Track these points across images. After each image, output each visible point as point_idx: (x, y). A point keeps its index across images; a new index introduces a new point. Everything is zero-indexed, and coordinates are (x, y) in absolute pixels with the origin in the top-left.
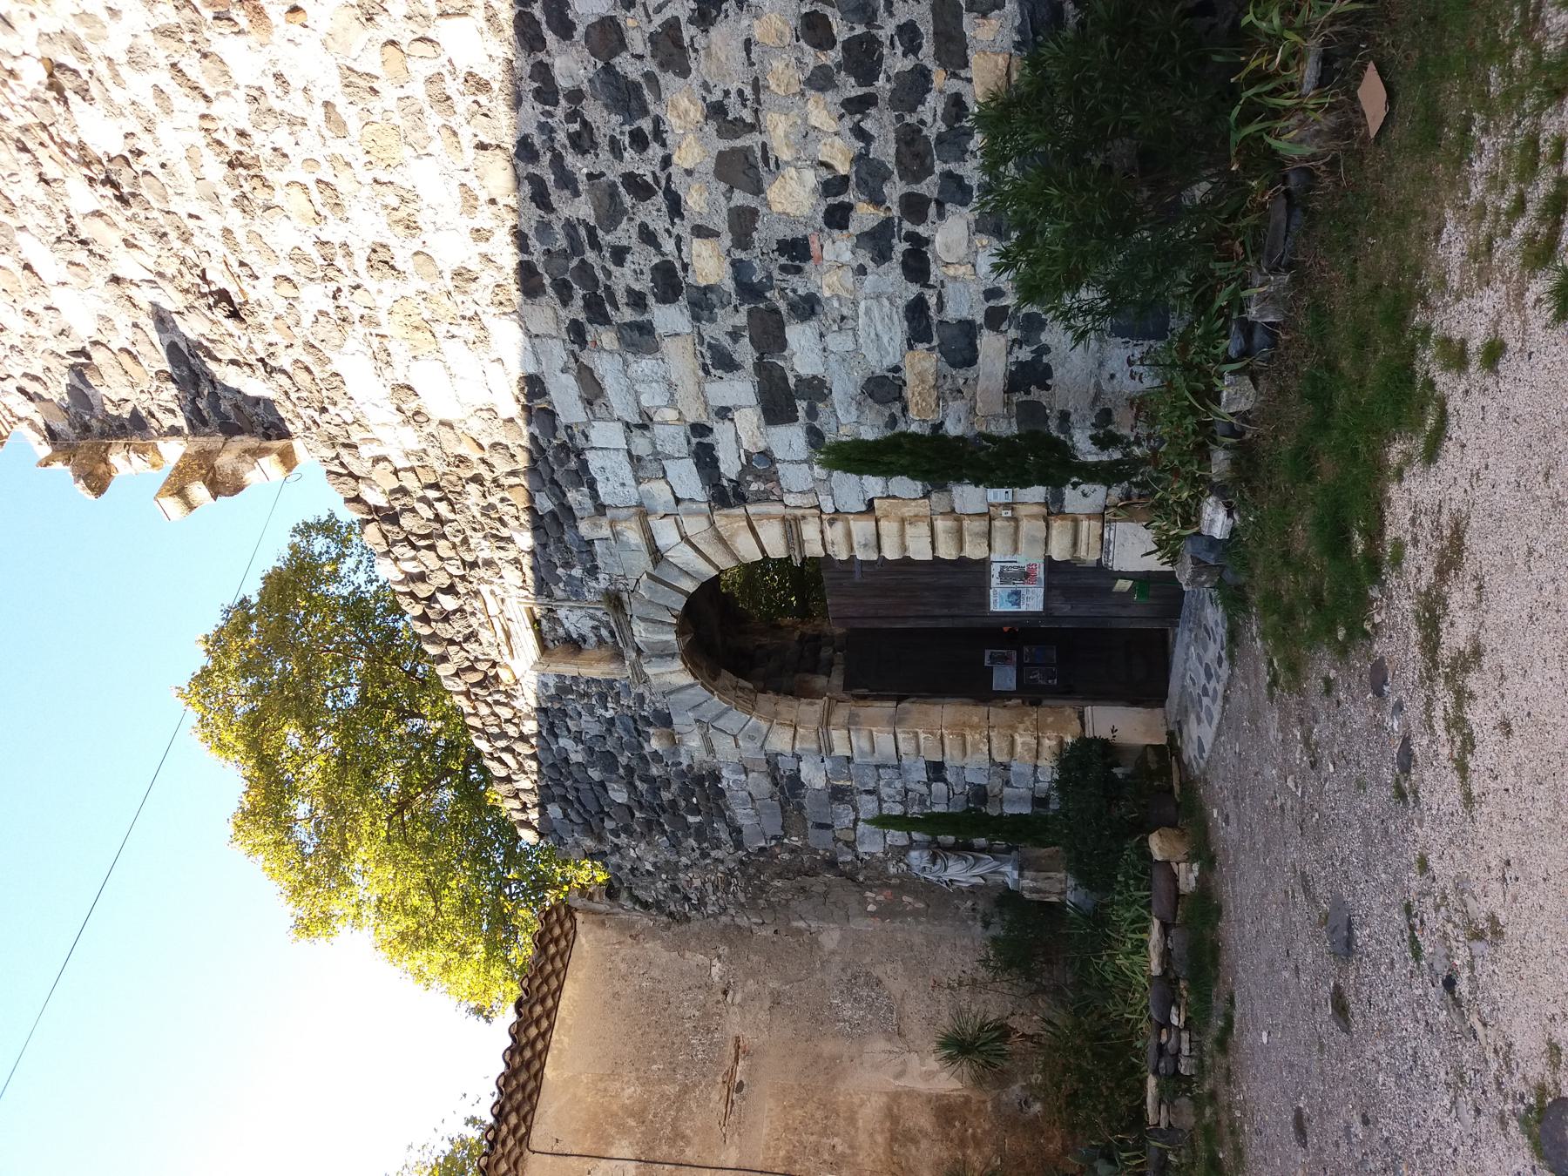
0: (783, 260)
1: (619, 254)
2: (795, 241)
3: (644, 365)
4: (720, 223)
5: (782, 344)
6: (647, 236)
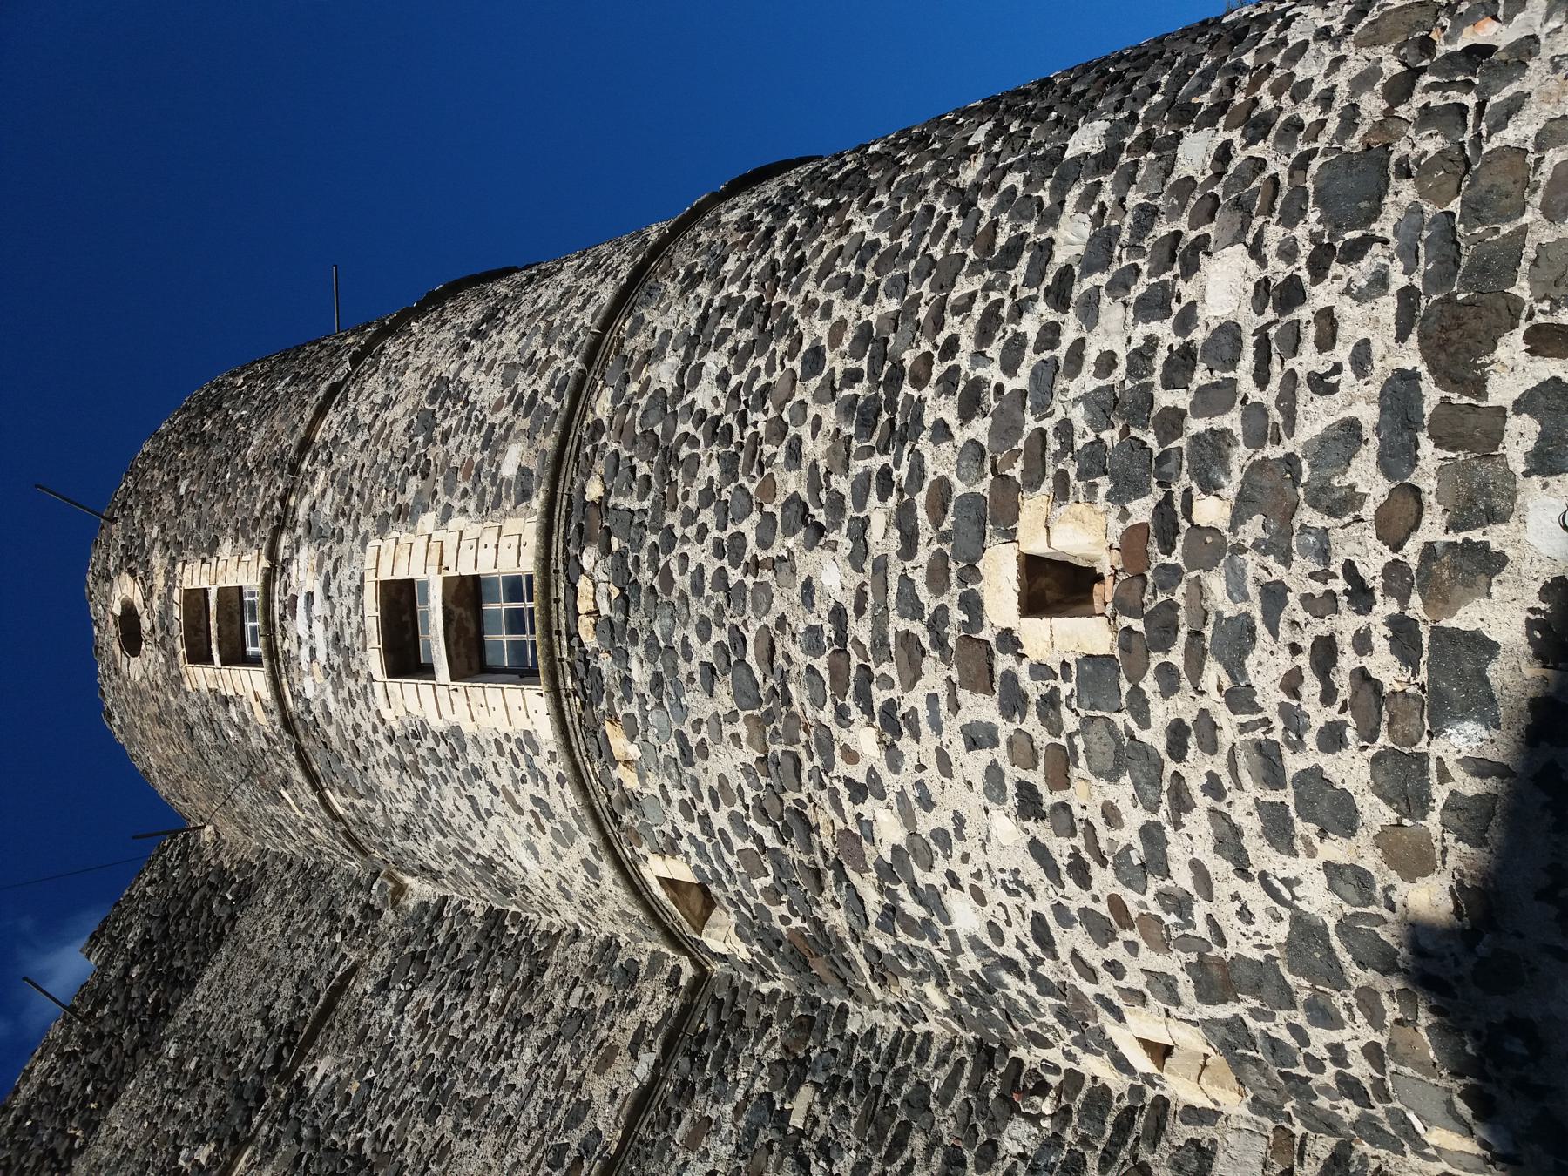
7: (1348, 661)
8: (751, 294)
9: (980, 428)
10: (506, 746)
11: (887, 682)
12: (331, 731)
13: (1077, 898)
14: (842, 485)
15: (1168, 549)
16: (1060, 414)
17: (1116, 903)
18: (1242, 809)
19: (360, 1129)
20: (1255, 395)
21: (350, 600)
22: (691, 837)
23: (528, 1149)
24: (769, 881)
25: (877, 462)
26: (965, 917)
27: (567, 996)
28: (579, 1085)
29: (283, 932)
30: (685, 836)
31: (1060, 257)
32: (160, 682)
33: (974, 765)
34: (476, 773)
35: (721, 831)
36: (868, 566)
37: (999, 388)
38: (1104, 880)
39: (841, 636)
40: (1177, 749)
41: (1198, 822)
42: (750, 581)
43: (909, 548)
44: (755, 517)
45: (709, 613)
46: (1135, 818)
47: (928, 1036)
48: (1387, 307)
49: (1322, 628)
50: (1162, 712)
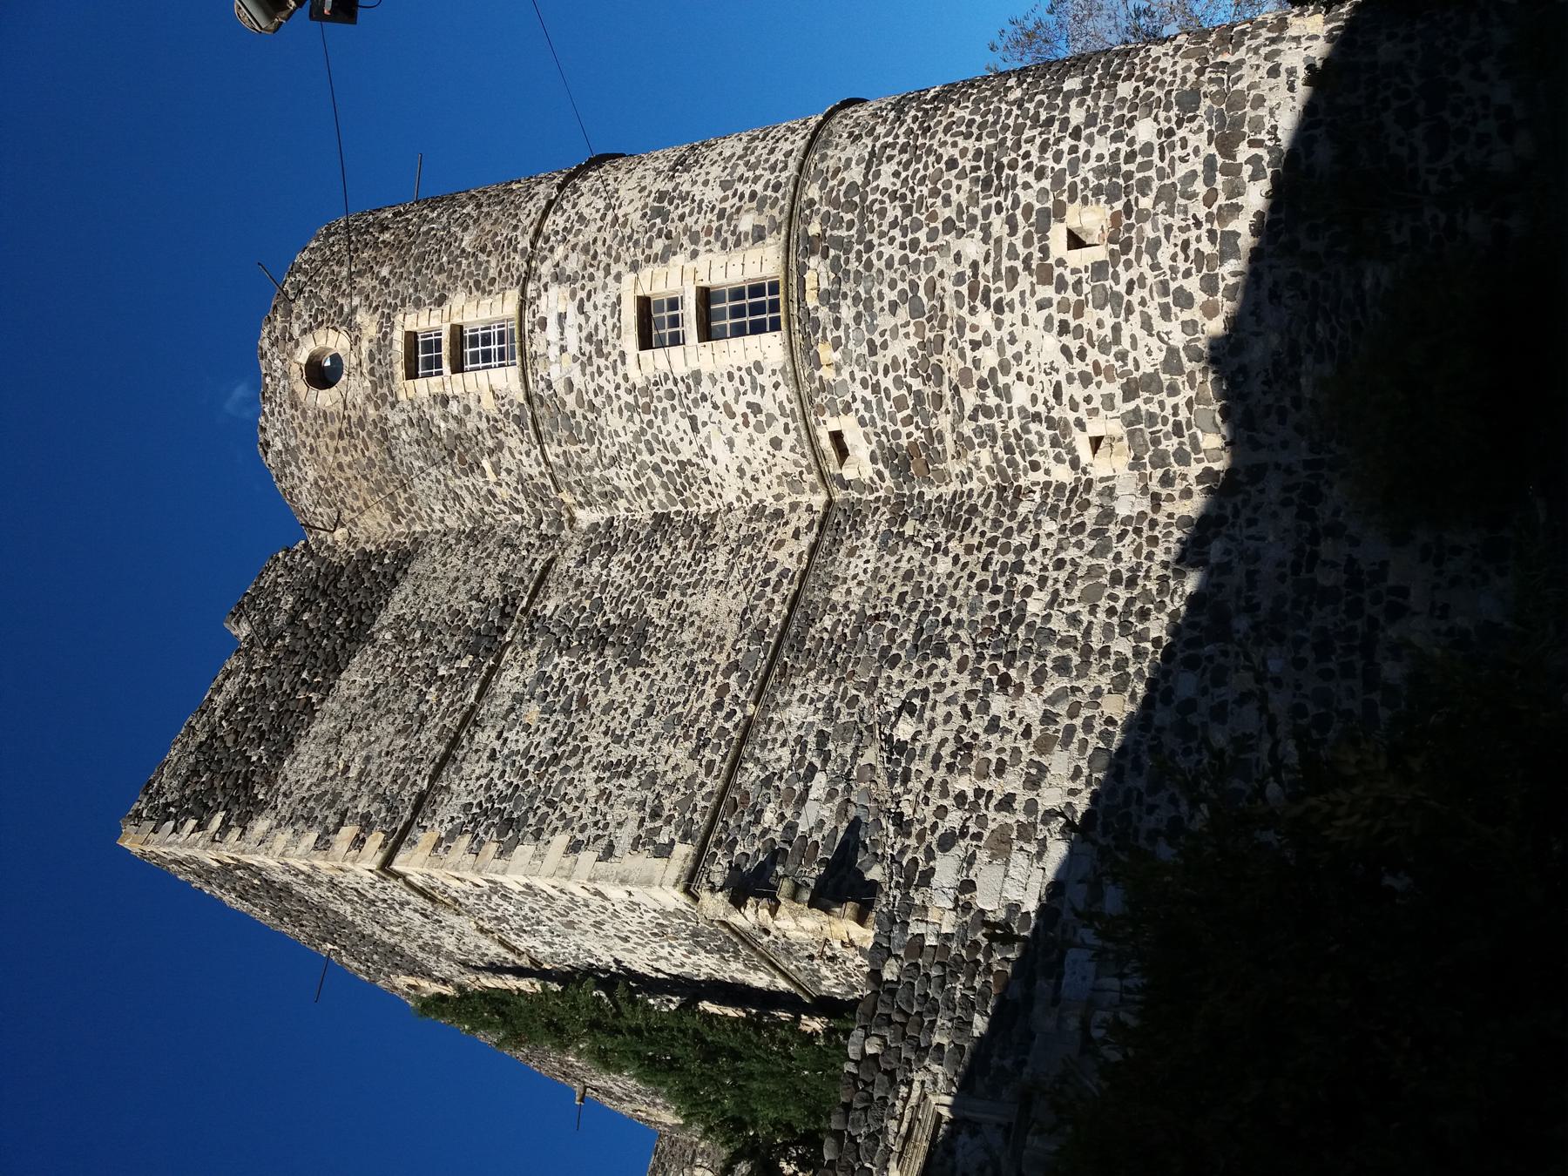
1: (1151, 809)
7: (1193, 246)
8: (902, 140)
9: (1046, 183)
10: (737, 375)
11: (999, 290)
12: (571, 400)
13: (1079, 366)
14: (976, 211)
15: (1129, 217)
16: (1082, 175)
17: (1096, 365)
18: (1153, 311)
20: (1160, 164)
21: (607, 312)
22: (864, 400)
24: (909, 412)
25: (994, 200)
26: (1021, 395)
27: (737, 532)
28: (765, 557)
31: (1073, 123)
33: (1038, 318)
34: (704, 398)
35: (886, 389)
36: (992, 242)
37: (1053, 168)
38: (1093, 354)
39: (975, 275)
40: (1129, 291)
41: (1136, 318)
42: (923, 258)
43: (1013, 230)
44: (925, 230)
45: (897, 276)
46: (1109, 322)
48: (1204, 135)
49: (1185, 236)
50: (1124, 277)
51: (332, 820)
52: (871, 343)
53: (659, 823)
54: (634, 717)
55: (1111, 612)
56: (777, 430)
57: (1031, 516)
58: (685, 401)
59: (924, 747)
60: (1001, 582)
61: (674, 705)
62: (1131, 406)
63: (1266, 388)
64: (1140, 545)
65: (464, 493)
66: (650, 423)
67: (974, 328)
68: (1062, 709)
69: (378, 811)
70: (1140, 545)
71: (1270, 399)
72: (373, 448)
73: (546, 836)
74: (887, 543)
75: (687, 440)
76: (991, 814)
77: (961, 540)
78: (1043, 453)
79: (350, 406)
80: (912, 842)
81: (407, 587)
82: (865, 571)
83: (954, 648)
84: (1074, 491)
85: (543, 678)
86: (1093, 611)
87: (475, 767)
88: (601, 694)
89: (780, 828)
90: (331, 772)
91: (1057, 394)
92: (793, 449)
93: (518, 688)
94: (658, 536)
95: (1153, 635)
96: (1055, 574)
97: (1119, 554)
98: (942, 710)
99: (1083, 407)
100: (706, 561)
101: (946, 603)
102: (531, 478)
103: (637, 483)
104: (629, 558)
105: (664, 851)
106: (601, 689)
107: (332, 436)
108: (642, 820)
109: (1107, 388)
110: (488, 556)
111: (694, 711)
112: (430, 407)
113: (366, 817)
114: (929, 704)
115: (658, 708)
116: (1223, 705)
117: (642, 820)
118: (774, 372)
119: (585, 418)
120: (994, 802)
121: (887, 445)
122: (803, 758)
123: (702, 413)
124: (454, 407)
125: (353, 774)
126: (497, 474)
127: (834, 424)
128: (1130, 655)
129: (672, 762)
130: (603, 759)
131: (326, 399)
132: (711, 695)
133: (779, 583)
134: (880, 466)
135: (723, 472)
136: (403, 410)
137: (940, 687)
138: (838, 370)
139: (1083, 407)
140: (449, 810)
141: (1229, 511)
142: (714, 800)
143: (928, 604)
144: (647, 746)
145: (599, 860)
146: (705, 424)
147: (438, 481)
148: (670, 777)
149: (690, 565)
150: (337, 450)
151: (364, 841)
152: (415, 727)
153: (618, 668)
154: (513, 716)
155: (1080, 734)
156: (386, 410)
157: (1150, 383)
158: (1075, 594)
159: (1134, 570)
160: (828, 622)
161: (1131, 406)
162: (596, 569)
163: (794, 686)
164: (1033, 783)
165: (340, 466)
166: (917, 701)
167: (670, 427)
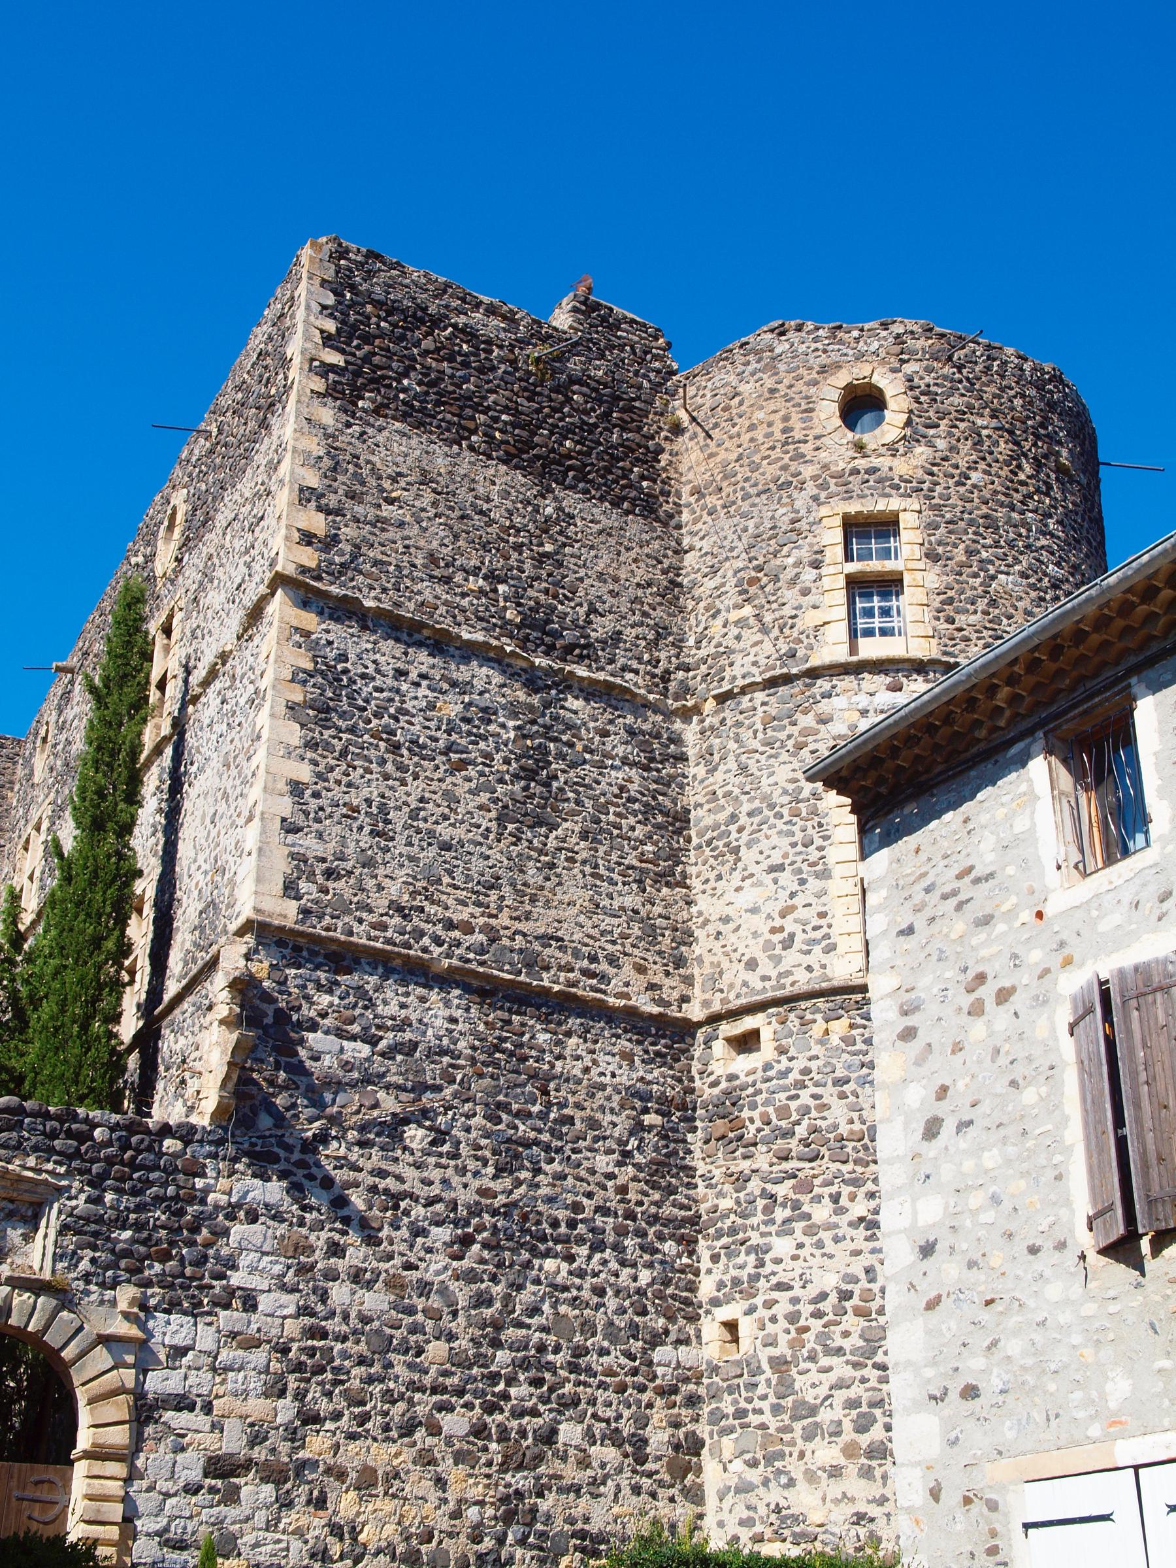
0: (316, 1493)
1: (329, 1394)
2: (325, 1502)
3: (256, 1384)
4: (341, 1459)
5: (265, 1480)
6: (337, 1416)
10: (823, 922)
13: (806, 1309)
17: (806, 1329)
18: (856, 1391)
19: (564, 771)
22: (789, 1070)
23: (591, 931)
24: (774, 1120)
26: (782, 1246)
27: (660, 916)
28: (626, 954)
29: (638, 585)
30: (791, 1064)
32: (822, 455)
33: (857, 1268)
34: (802, 882)
35: (797, 1097)
38: (816, 1325)
40: (877, 1366)
41: (848, 1372)
46: (847, 1344)
47: (696, 1187)
51: (332, 501)
52: (847, 1081)
53: (320, 879)
54: (439, 828)
55: (541, 1348)
56: (766, 967)
57: (659, 1256)
58: (799, 858)
59: (396, 1160)
60: (581, 1229)
61: (450, 873)
62: (765, 1366)
63: (772, 1507)
64: (615, 1375)
65: (718, 580)
66: (779, 816)
67: (853, 1197)
68: (435, 1302)
69: (341, 553)
70: (615, 1375)
71: (762, 1510)
72: (772, 471)
73: (309, 755)
74: (639, 1097)
75: (761, 858)
76: (324, 1235)
77: (635, 1179)
78: (725, 1272)
79: (818, 443)
80: (296, 1156)
81: (611, 519)
82: (602, 1074)
83: (507, 1182)
84: (687, 1302)
85: (488, 714)
86: (544, 1329)
87: (389, 652)
88: (467, 785)
89: (313, 1014)
90: (386, 484)
91: (781, 1287)
92: (745, 984)
93: (478, 684)
94: (660, 819)
95: (513, 1391)
96: (587, 1286)
97: (608, 1353)
98: (436, 1175)
99: (767, 1314)
100: (624, 884)
101: (559, 1169)
102: (731, 665)
103: (720, 793)
104: (634, 788)
105: (290, 889)
106: (473, 785)
107: (786, 419)
108: (324, 860)
109: (783, 1339)
110: (645, 614)
111: (444, 897)
112: (811, 545)
113: (335, 539)
114: (443, 1161)
115: (448, 855)
116: (433, 1462)
117: (324, 860)
118: (824, 967)
119: (789, 737)
120: (337, 1237)
121: (744, 1094)
122: (388, 1029)
123: (787, 879)
124: (809, 574)
125: (387, 511)
126: (736, 623)
127: (766, 1035)
128: (493, 1368)
129: (387, 883)
130: (391, 804)
131: (828, 411)
132: (461, 914)
133: (593, 975)
134: (724, 1085)
135: (727, 898)
136: (809, 511)
137: (462, 1171)
138: (821, 1042)
139: (767, 1314)
140: (340, 634)
141: (650, 1466)
142: (343, 938)
143: (559, 1150)
144: (405, 850)
145: (284, 820)
146: (776, 881)
147: (732, 549)
148: (370, 884)
149: (619, 864)
150: (770, 425)
151: (309, 544)
152: (437, 573)
153: (496, 801)
154: (446, 686)
155: (407, 1320)
156: (811, 489)
157: (785, 1387)
158: (563, 1309)
159: (589, 1371)
160: (542, 1038)
161: (765, 1366)
162: (620, 750)
163: (467, 1010)
164: (356, 1277)
165: (752, 427)
166: (446, 1148)
167: (775, 840)
